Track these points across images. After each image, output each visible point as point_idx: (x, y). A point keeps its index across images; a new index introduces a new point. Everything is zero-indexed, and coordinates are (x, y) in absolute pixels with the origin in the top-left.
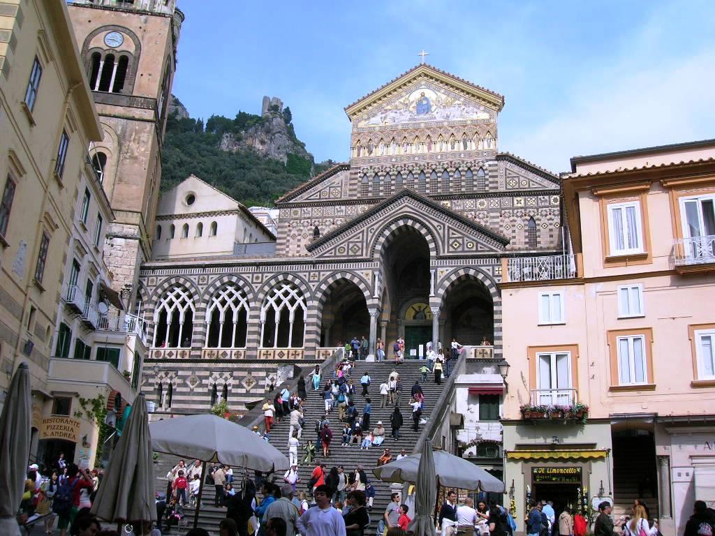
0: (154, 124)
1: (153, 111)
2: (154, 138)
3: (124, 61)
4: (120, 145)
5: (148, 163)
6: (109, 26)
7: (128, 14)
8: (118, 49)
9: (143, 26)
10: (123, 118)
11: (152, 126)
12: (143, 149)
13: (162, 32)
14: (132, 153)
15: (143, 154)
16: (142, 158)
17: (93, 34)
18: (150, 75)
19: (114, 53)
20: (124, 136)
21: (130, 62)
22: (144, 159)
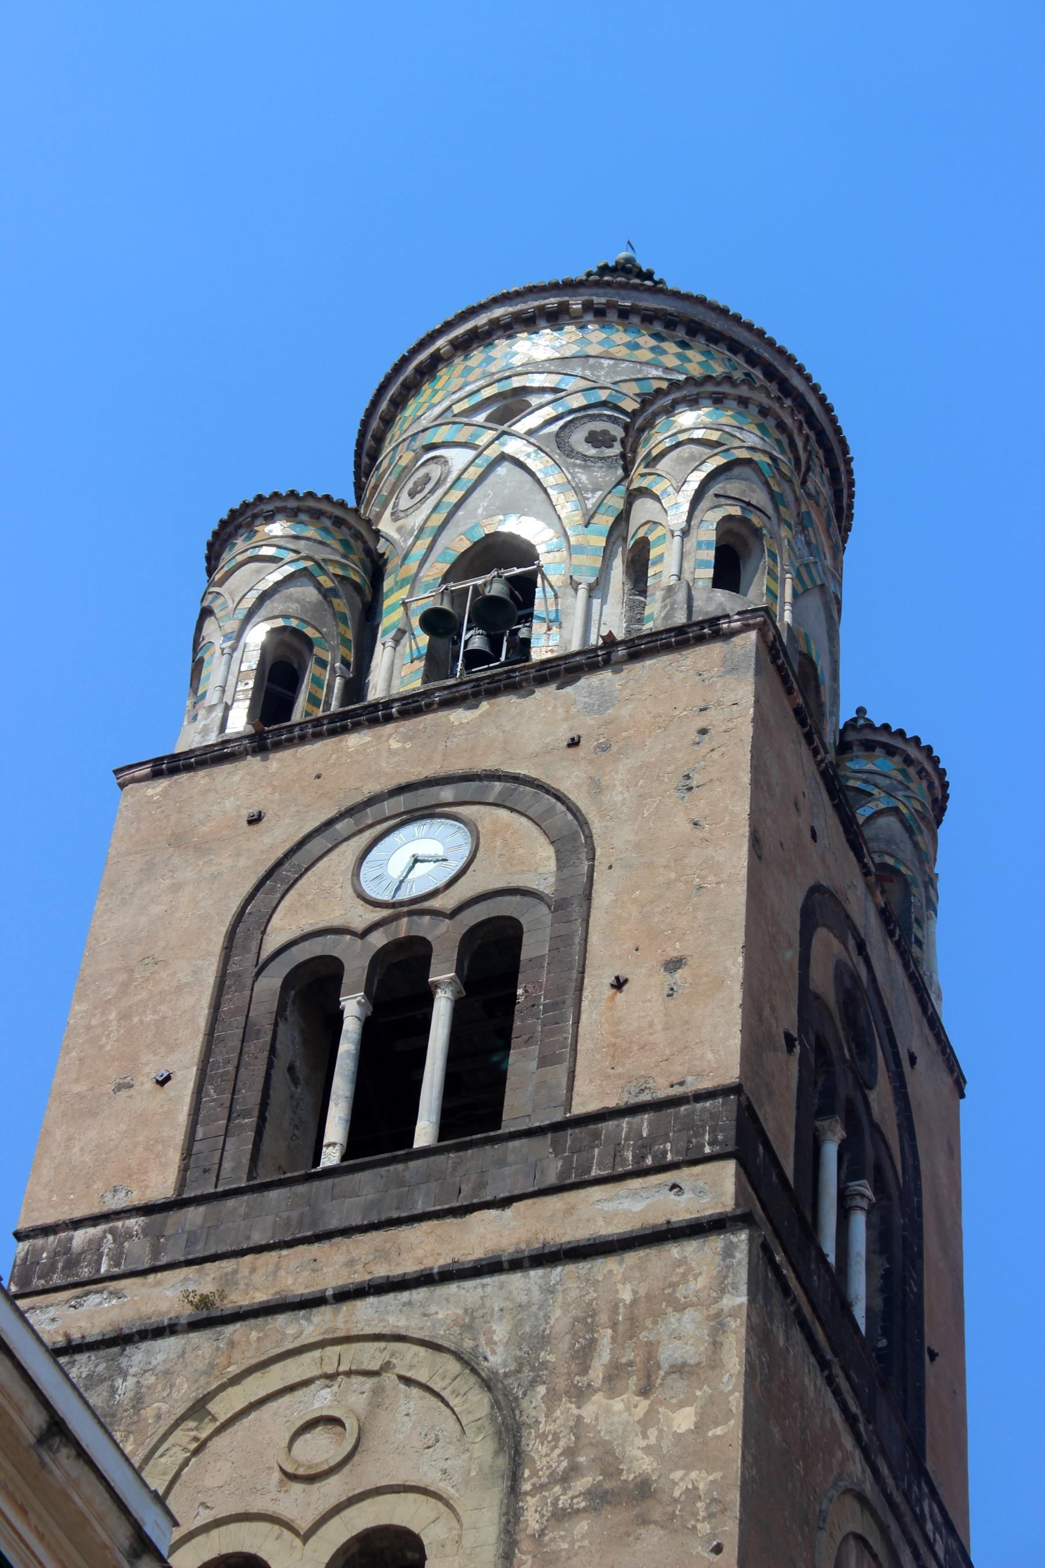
0: (742, 1238)
1: (730, 1167)
2: (759, 1336)
3: (493, 954)
4: (510, 1437)
5: (734, 1497)
6: (373, 800)
7: (485, 706)
8: (446, 902)
9: (587, 725)
10: (517, 1264)
11: (728, 1252)
12: (684, 1420)
13: (714, 718)
14: (609, 1462)
15: (693, 1450)
16: (681, 1480)
17: (280, 876)
18: (674, 965)
19: (423, 927)
20: (539, 1373)
21: (534, 946)
22: (701, 1479)
